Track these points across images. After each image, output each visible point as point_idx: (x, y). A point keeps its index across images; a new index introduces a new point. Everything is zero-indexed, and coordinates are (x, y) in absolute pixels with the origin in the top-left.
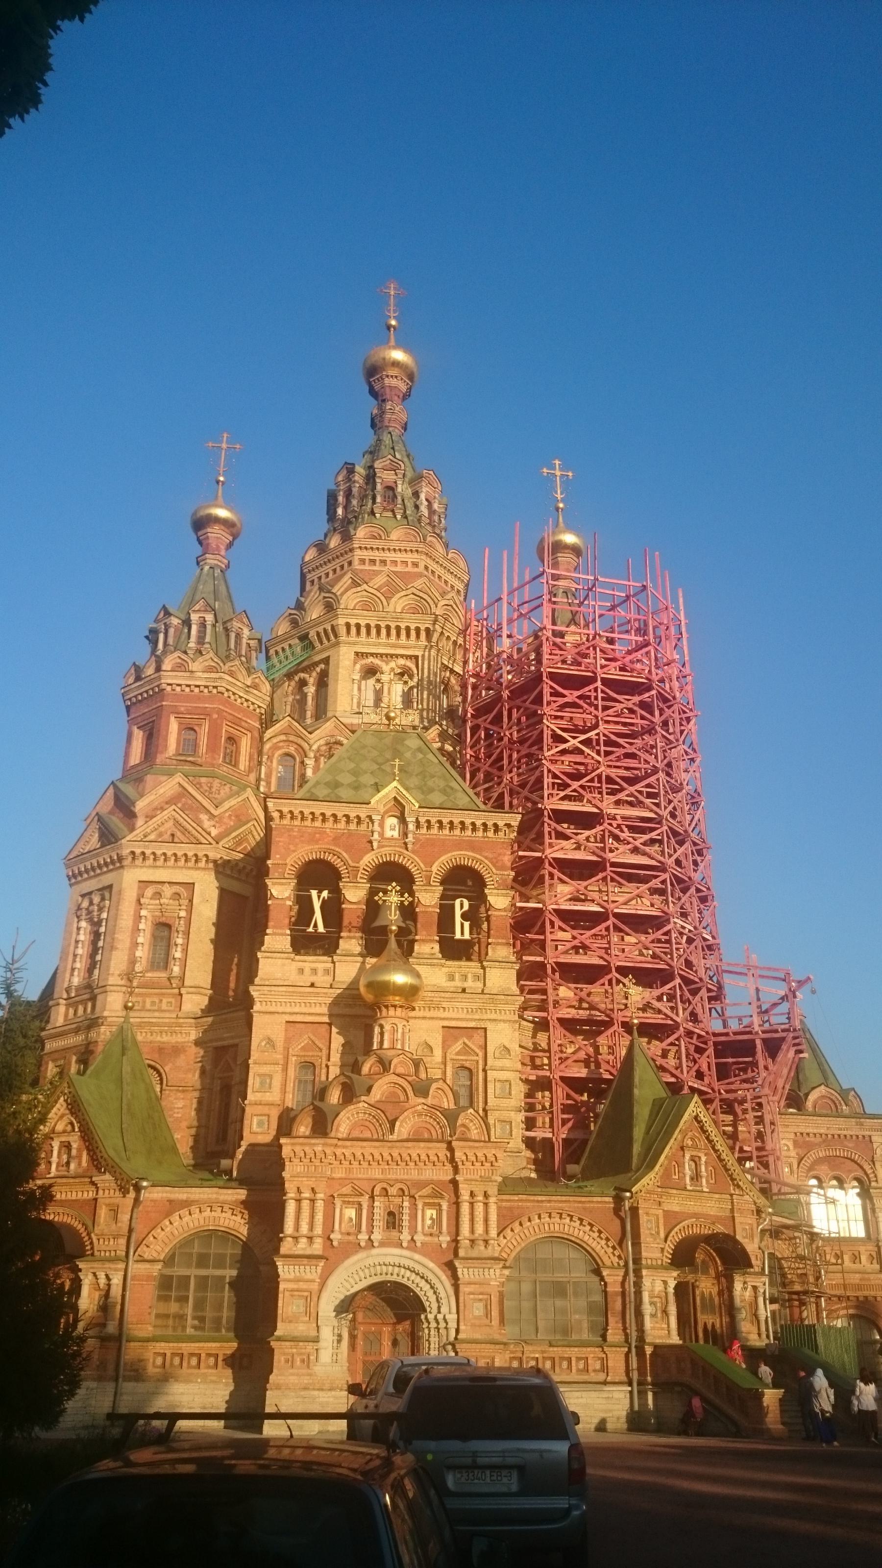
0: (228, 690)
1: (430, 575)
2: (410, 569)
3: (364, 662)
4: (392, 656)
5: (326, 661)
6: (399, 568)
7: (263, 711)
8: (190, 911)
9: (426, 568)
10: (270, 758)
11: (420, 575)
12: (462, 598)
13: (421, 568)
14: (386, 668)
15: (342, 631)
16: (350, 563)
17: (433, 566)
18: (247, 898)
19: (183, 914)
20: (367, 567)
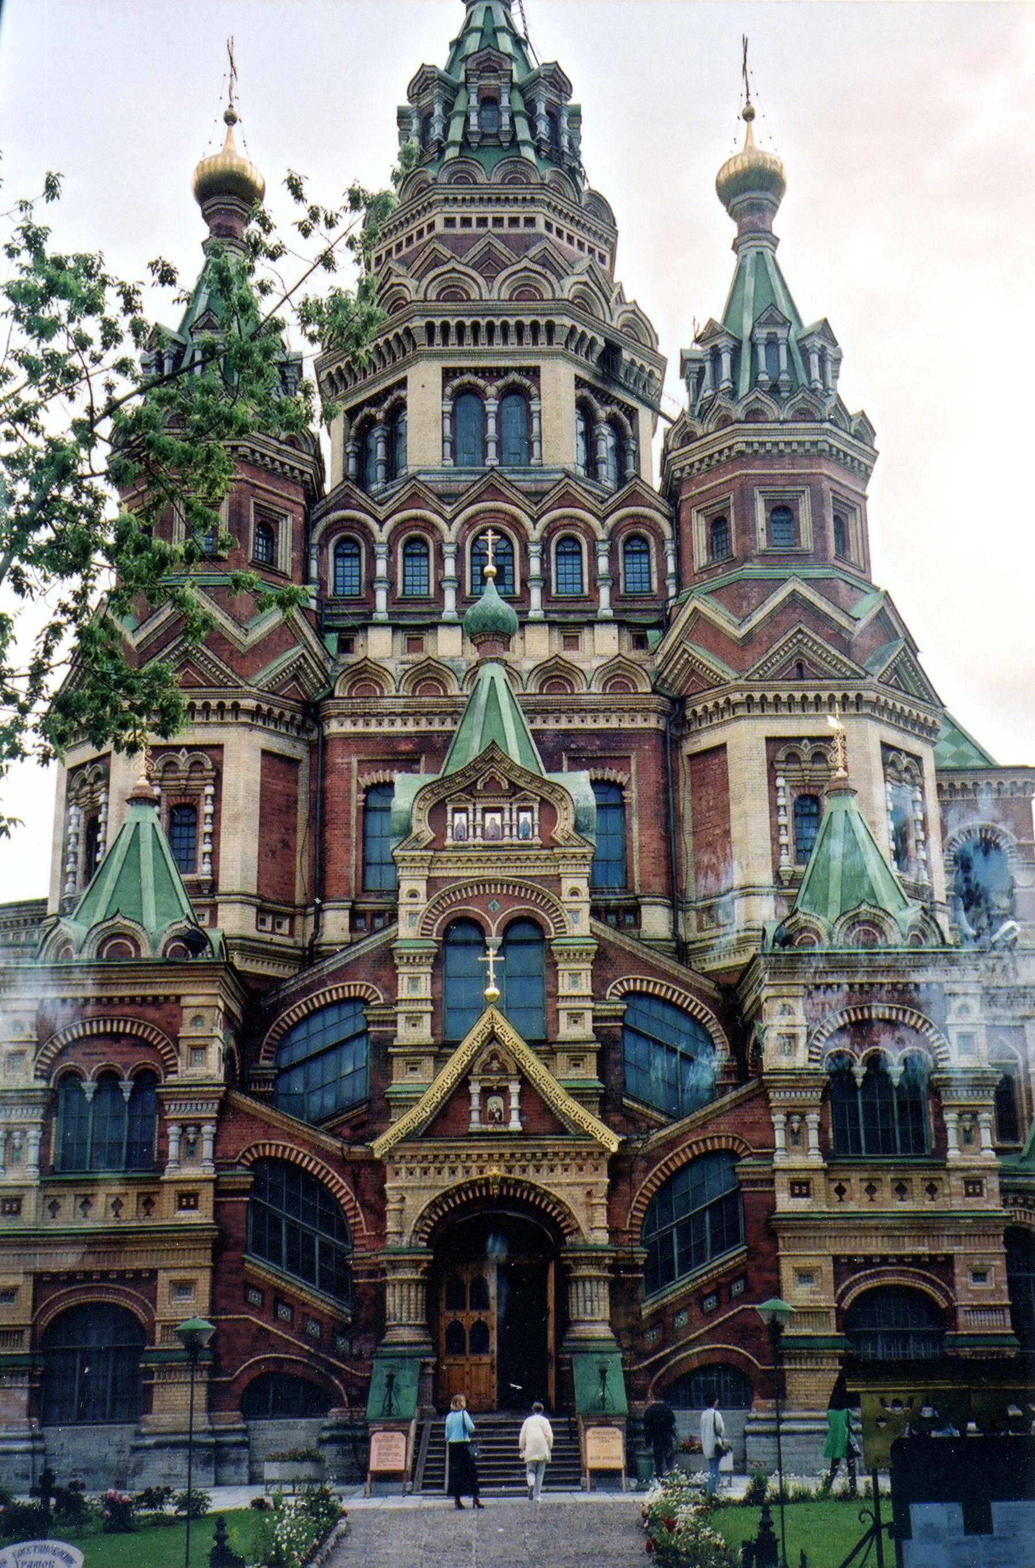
0: (253, 451)
1: (553, 236)
2: (522, 229)
3: (456, 382)
4: (498, 370)
5: (402, 384)
6: (506, 230)
7: (307, 477)
8: (218, 782)
9: (548, 226)
10: (322, 546)
11: (540, 237)
12: (606, 267)
13: (540, 227)
14: (491, 390)
15: (421, 338)
16: (431, 227)
17: (557, 222)
19: (210, 790)
20: (458, 230)
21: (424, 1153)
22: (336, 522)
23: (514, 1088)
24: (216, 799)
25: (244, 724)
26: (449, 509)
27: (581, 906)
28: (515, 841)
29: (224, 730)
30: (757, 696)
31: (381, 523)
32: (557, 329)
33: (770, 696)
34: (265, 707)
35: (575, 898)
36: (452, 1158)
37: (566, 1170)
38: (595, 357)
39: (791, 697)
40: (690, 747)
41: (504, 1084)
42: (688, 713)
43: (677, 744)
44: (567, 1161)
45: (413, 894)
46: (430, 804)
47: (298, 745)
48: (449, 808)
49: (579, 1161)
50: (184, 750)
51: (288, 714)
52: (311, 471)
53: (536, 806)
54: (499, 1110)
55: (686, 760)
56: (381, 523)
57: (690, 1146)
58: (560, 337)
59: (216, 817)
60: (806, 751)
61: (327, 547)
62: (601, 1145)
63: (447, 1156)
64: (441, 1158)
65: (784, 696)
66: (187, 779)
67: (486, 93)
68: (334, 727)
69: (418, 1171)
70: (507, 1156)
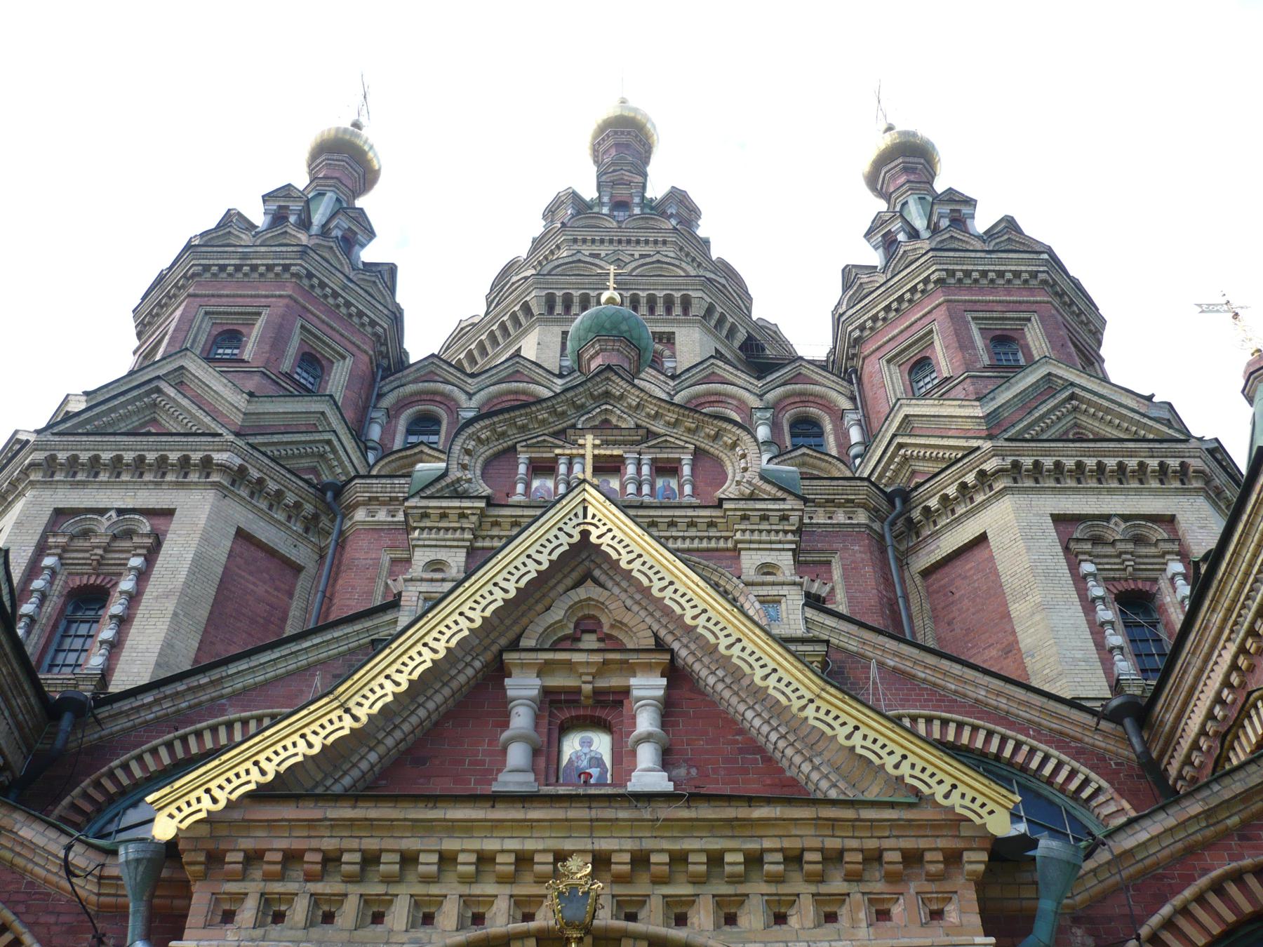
0: (310, 275)
8: (152, 553)
18: (298, 569)
21: (329, 844)
22: (412, 395)
23: (648, 687)
24: (143, 576)
25: (216, 485)
26: (560, 382)
27: (784, 590)
28: (647, 499)
29: (182, 493)
30: (1027, 462)
31: (470, 396)
32: (694, 301)
33: (1048, 462)
34: (255, 474)
35: (769, 578)
36: (428, 863)
37: (831, 918)
38: (737, 344)
39: (1080, 465)
40: (923, 560)
41: (615, 682)
42: (916, 514)
43: (902, 564)
44: (837, 885)
45: (436, 565)
46: (486, 452)
47: (301, 547)
48: (523, 457)
49: (878, 887)
50: (113, 513)
51: (290, 499)
52: (386, 326)
53: (687, 458)
54: (598, 761)
55: (918, 579)
56: (470, 396)
57: (1217, 888)
58: (697, 310)
59: (133, 599)
60: (1117, 530)
61: (397, 416)
62: (957, 822)
63: (409, 859)
64: (389, 864)
65: (1070, 463)
66: (106, 550)
67: (619, 199)
68: (360, 515)
69: (299, 911)
70: (621, 863)
